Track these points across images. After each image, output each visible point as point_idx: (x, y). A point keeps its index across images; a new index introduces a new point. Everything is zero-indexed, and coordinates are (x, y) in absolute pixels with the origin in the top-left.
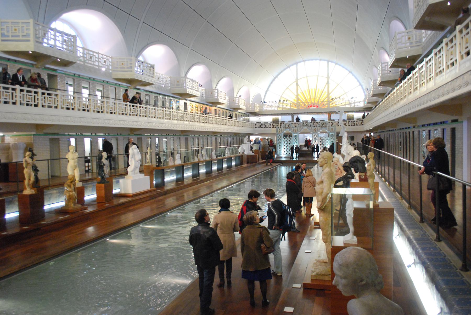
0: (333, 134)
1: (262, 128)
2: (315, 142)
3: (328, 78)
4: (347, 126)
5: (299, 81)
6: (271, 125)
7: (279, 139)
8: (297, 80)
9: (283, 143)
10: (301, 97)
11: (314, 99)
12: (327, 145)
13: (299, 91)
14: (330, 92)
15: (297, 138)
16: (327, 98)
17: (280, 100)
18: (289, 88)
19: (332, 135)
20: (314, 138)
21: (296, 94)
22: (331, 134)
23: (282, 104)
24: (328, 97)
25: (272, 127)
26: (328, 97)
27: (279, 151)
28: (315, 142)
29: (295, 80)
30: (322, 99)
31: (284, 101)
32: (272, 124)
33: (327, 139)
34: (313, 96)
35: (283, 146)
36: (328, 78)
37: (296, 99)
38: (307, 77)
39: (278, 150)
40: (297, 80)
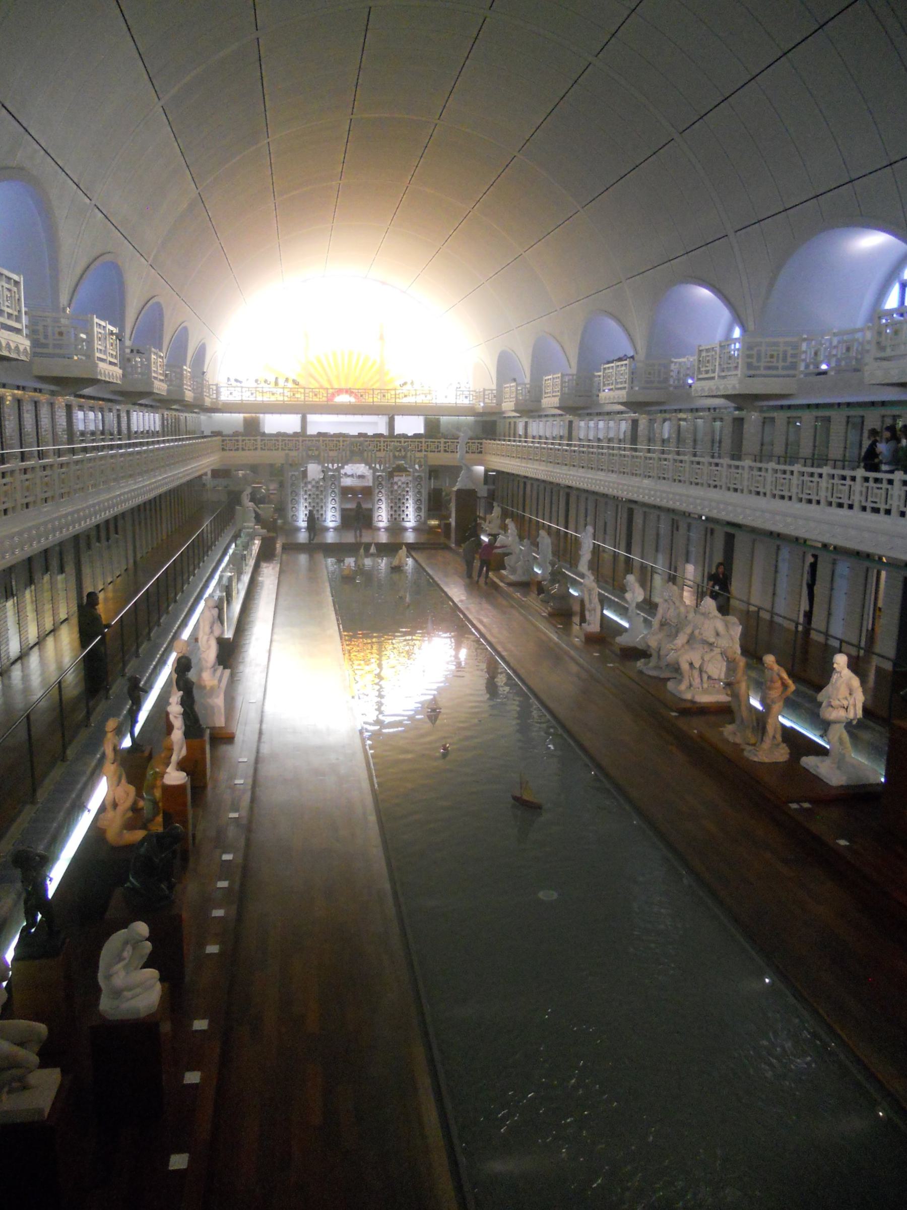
0: (423, 475)
1: (237, 449)
2: (380, 492)
4: (440, 451)
6: (259, 442)
7: (293, 485)
9: (302, 493)
12: (407, 499)
15: (336, 483)
17: (277, 379)
19: (419, 476)
20: (377, 483)
22: (416, 474)
23: (283, 388)
25: (262, 449)
27: (292, 514)
28: (380, 492)
31: (287, 380)
32: (262, 440)
33: (407, 487)
35: (302, 501)
39: (290, 511)
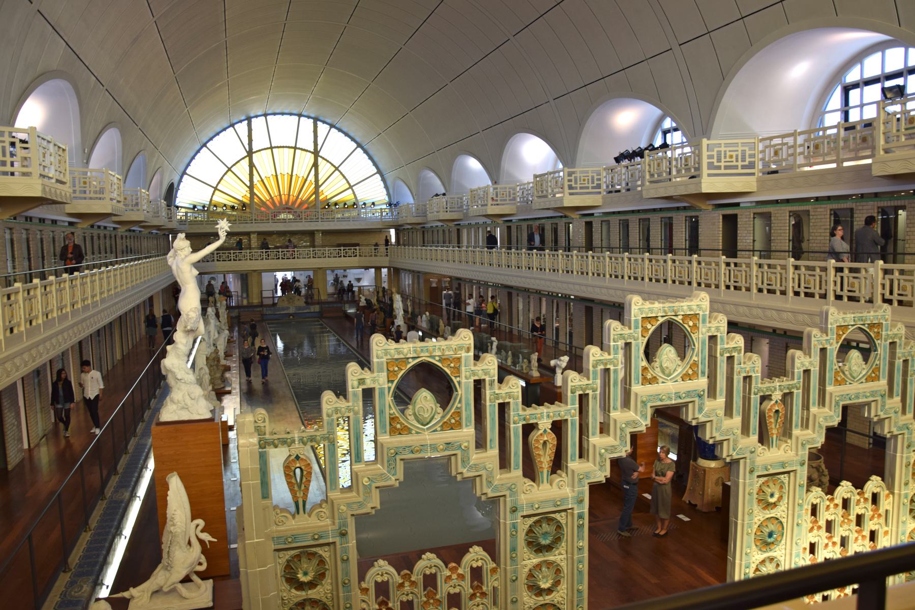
3: (316, 153)
5: (254, 155)
8: (250, 153)
10: (260, 191)
11: (287, 196)
13: (256, 178)
14: (320, 183)
16: (314, 196)
18: (232, 169)
21: (248, 185)
24: (316, 191)
26: (316, 191)
29: (246, 154)
30: (304, 195)
34: (284, 190)
36: (316, 153)
37: (248, 195)
38: (271, 148)
40: (250, 153)
